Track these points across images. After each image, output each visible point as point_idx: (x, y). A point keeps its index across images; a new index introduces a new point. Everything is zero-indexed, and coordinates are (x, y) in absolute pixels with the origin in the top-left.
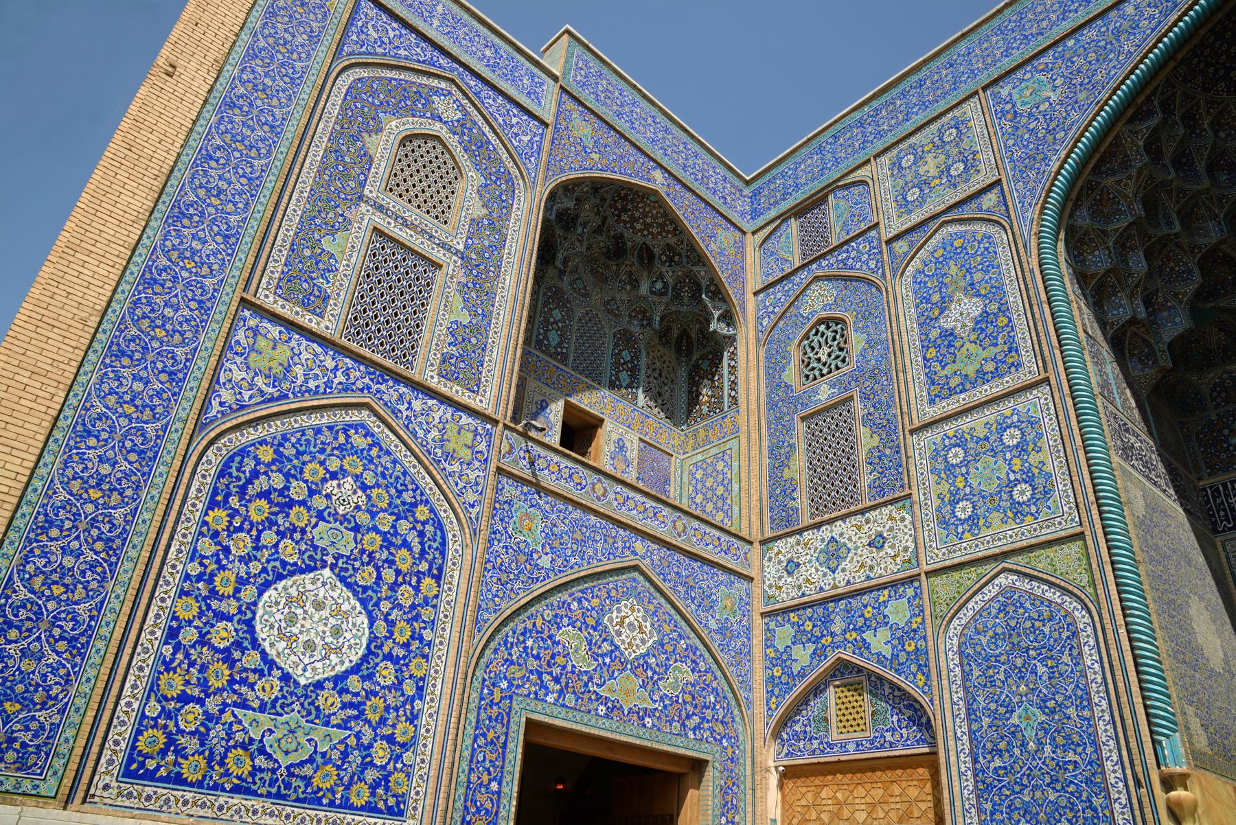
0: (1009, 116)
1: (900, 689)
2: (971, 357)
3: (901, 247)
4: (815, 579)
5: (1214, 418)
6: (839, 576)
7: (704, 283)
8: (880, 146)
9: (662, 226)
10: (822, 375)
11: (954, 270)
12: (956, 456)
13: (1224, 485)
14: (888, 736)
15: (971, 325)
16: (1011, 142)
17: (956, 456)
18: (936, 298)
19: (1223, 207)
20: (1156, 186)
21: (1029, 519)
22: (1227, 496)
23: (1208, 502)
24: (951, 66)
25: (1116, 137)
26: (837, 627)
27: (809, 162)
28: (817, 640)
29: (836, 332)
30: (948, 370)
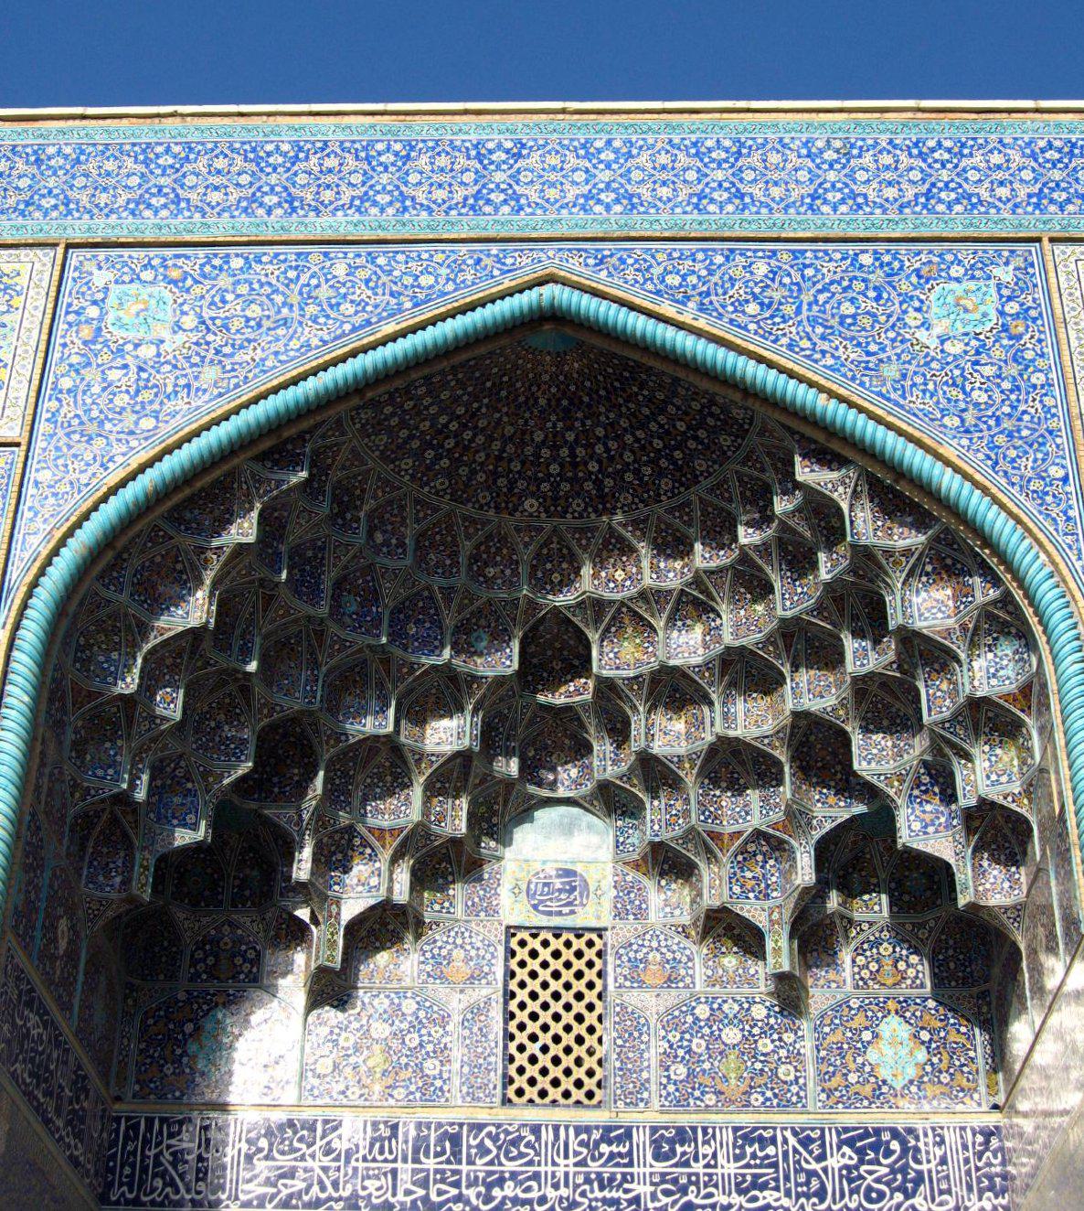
0: (86, 332)
5: (182, 996)
13: (150, 1122)
19: (331, 656)
20: (252, 582)
22: (146, 1142)
23: (114, 1143)
25: (231, 474)
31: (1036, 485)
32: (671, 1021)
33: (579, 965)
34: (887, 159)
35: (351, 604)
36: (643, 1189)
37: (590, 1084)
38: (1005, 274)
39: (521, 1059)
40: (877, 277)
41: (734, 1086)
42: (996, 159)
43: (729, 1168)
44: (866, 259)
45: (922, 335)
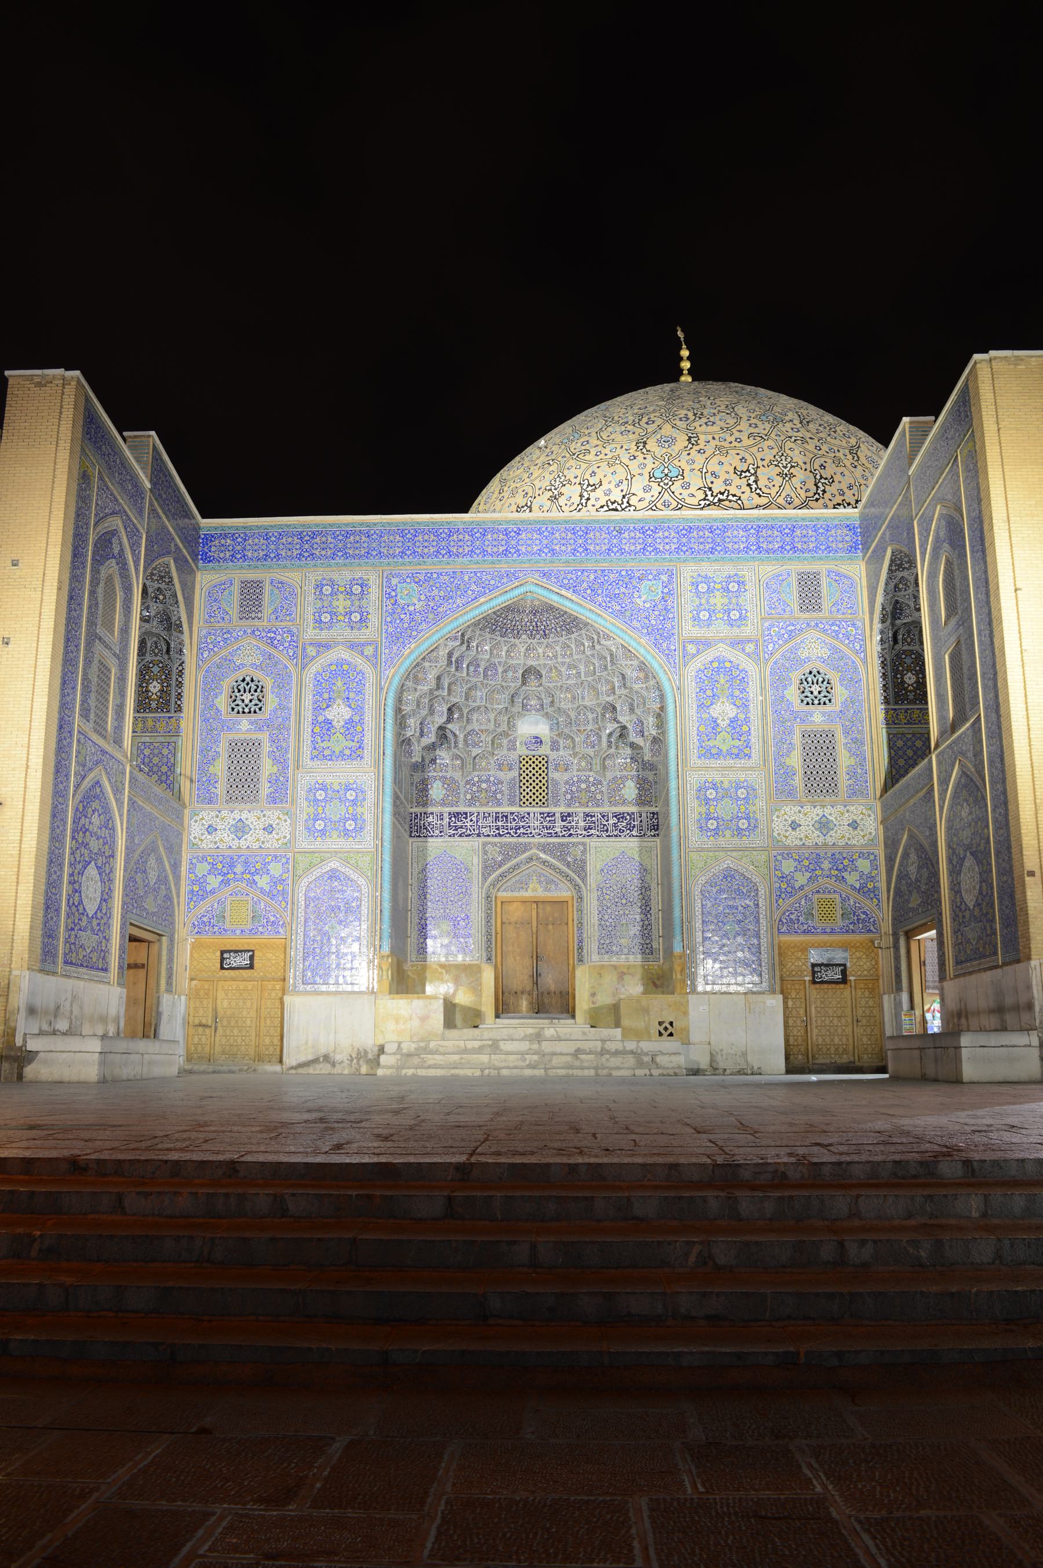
0: (393, 601)
2: (338, 743)
3: (311, 651)
4: (225, 838)
7: (174, 619)
9: (162, 577)
10: (244, 712)
11: (339, 684)
12: (320, 795)
14: (260, 929)
15: (343, 723)
16: (389, 619)
17: (320, 795)
18: (326, 696)
21: (351, 839)
26: (239, 869)
28: (225, 874)
30: (325, 744)
31: (667, 652)
32: (567, 783)
33: (540, 765)
34: (632, 534)
35: (472, 669)
36: (558, 830)
37: (543, 800)
38: (664, 578)
39: (524, 794)
40: (627, 580)
41: (584, 801)
42: (666, 534)
43: (582, 824)
44: (624, 573)
45: (638, 600)
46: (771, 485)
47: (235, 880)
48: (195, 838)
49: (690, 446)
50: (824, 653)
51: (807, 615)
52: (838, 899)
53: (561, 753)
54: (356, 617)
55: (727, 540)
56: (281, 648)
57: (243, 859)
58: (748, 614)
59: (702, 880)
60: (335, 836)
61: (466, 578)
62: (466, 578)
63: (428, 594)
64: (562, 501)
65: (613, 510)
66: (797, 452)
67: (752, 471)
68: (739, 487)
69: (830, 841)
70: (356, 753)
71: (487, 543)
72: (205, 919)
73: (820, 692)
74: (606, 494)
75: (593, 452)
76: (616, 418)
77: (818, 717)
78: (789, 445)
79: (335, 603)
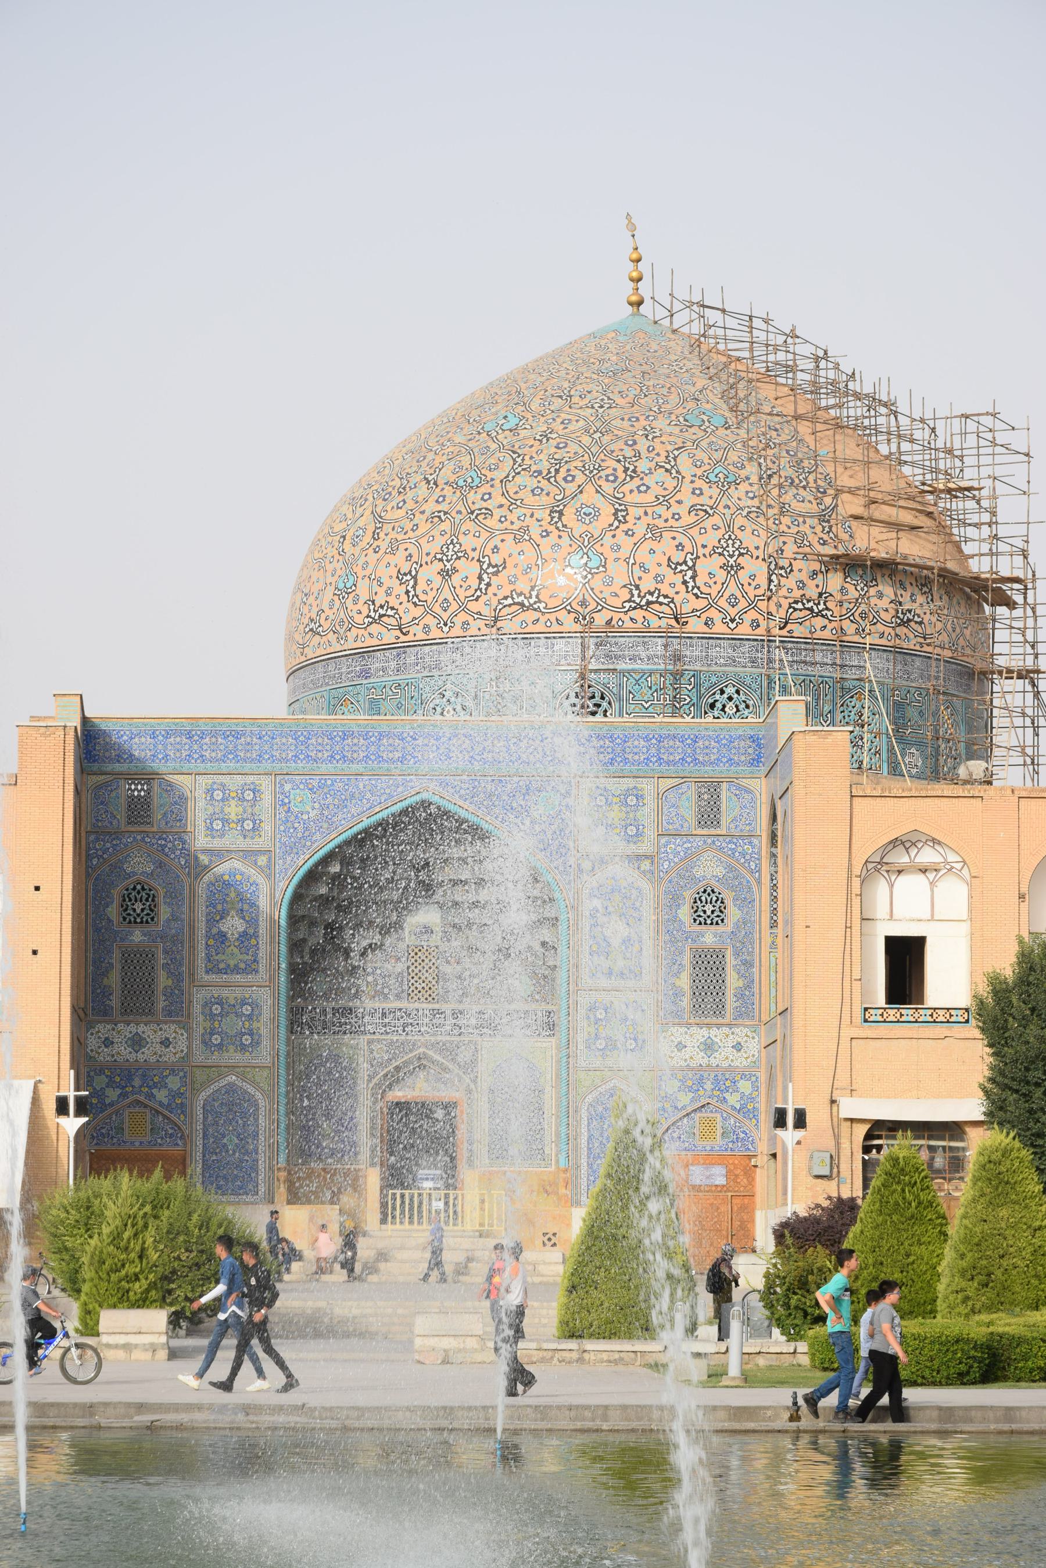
1: (168, 1118)
2: (233, 955)
4: (123, 1052)
6: (140, 1056)
8: (201, 767)
10: (135, 922)
12: (216, 1009)
14: (159, 1141)
15: (237, 936)
16: (282, 828)
17: (216, 1009)
18: (219, 907)
21: (247, 1054)
24: (260, 738)
26: (137, 1082)
27: (143, 740)
28: (123, 1088)
29: (149, 895)
30: (220, 957)
46: (711, 584)
47: (133, 1093)
48: (92, 1051)
49: (616, 523)
50: (720, 871)
51: (705, 832)
52: (719, 1119)
53: (454, 944)
54: (248, 825)
55: (628, 750)
56: (173, 856)
57: (140, 1072)
58: (645, 830)
59: (589, 1099)
60: (232, 1051)
61: (361, 786)
62: (361, 786)
63: (322, 802)
64: (456, 579)
65: (518, 604)
66: (749, 530)
67: (690, 563)
68: (672, 585)
69: (714, 1062)
70: (250, 968)
71: (382, 748)
72: (103, 1131)
73: (713, 912)
74: (511, 582)
75: (496, 517)
76: (527, 461)
77: (709, 937)
78: (740, 521)
79: (227, 810)
